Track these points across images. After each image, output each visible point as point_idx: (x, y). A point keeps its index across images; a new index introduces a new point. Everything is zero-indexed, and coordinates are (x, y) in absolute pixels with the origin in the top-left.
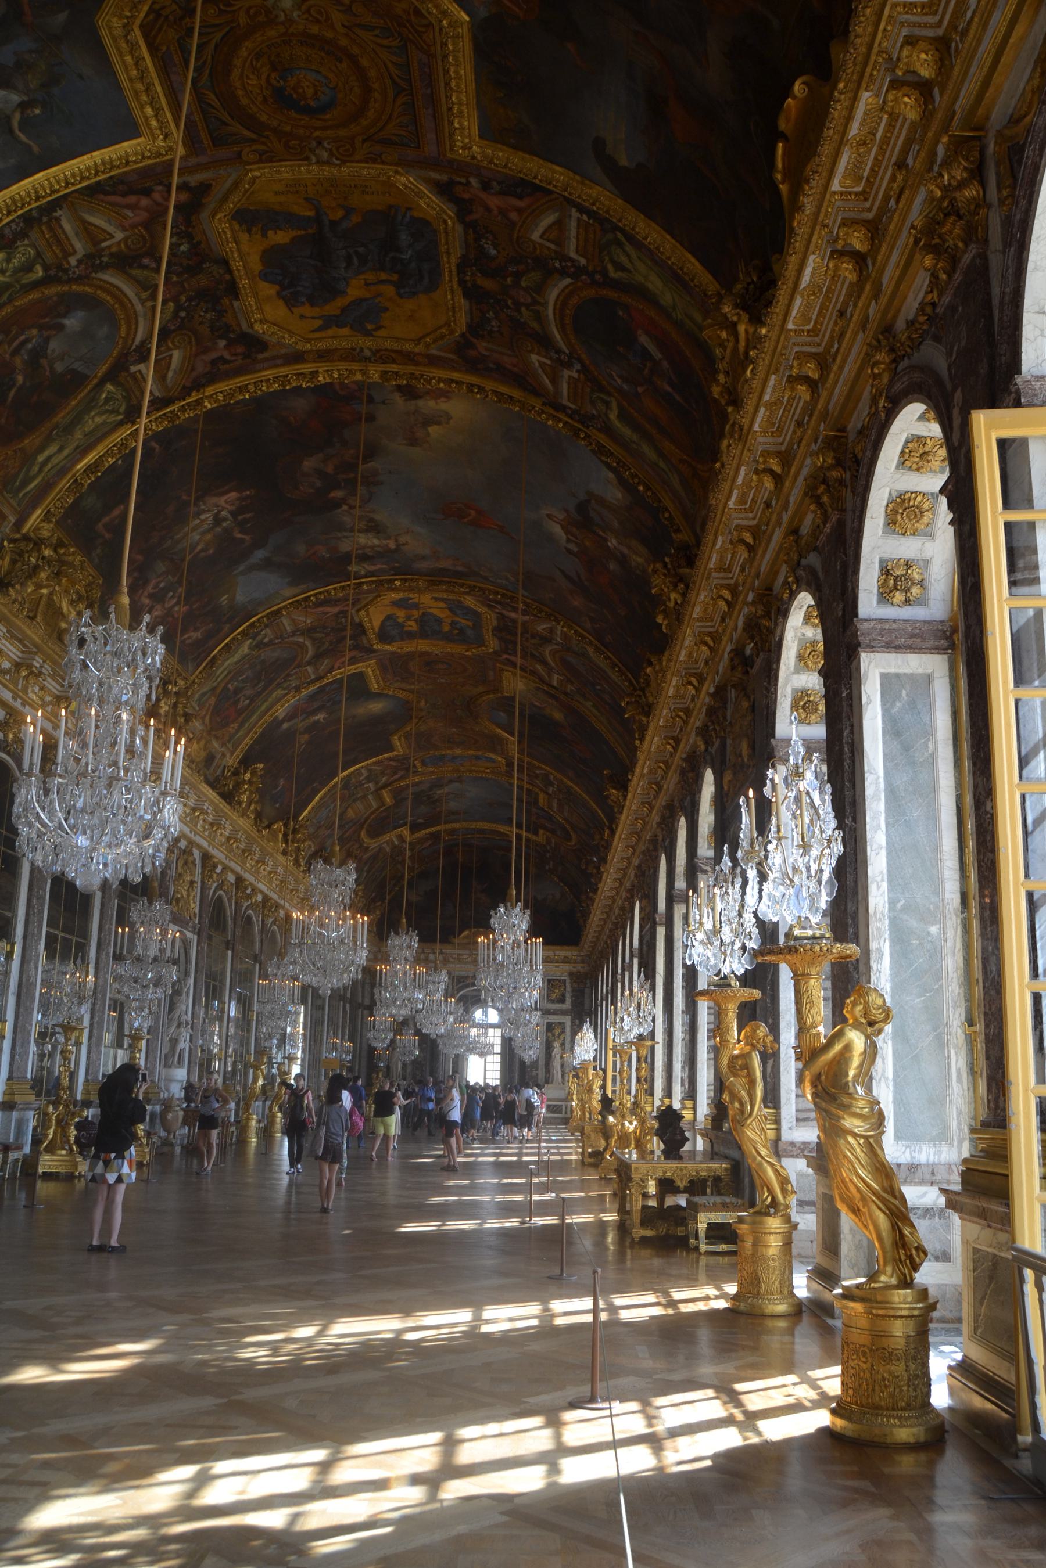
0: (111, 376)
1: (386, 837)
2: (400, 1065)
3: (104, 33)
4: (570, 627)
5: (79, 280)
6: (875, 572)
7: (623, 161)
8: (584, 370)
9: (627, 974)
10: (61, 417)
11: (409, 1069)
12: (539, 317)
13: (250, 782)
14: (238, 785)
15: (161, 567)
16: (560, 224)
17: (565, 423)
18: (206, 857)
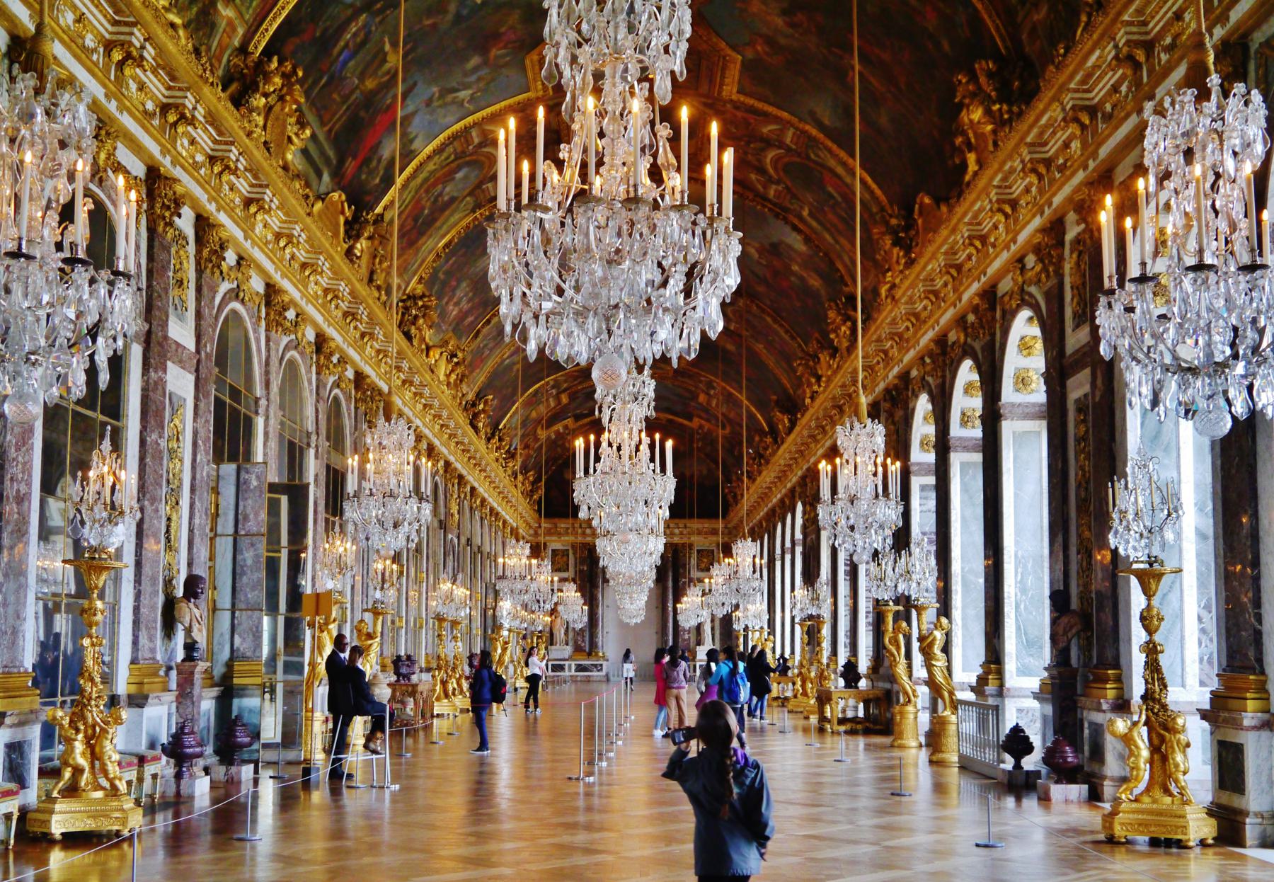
0: (470, 194)
1: (555, 428)
2: (563, 631)
3: (528, 62)
4: (752, 302)
5: (471, 155)
6: (959, 414)
7: (827, 122)
8: (787, 188)
9: (788, 557)
10: (438, 224)
11: (571, 635)
12: (759, 161)
13: (484, 411)
14: (476, 416)
15: (464, 285)
16: (781, 130)
17: (770, 209)
18: (461, 477)
